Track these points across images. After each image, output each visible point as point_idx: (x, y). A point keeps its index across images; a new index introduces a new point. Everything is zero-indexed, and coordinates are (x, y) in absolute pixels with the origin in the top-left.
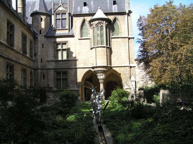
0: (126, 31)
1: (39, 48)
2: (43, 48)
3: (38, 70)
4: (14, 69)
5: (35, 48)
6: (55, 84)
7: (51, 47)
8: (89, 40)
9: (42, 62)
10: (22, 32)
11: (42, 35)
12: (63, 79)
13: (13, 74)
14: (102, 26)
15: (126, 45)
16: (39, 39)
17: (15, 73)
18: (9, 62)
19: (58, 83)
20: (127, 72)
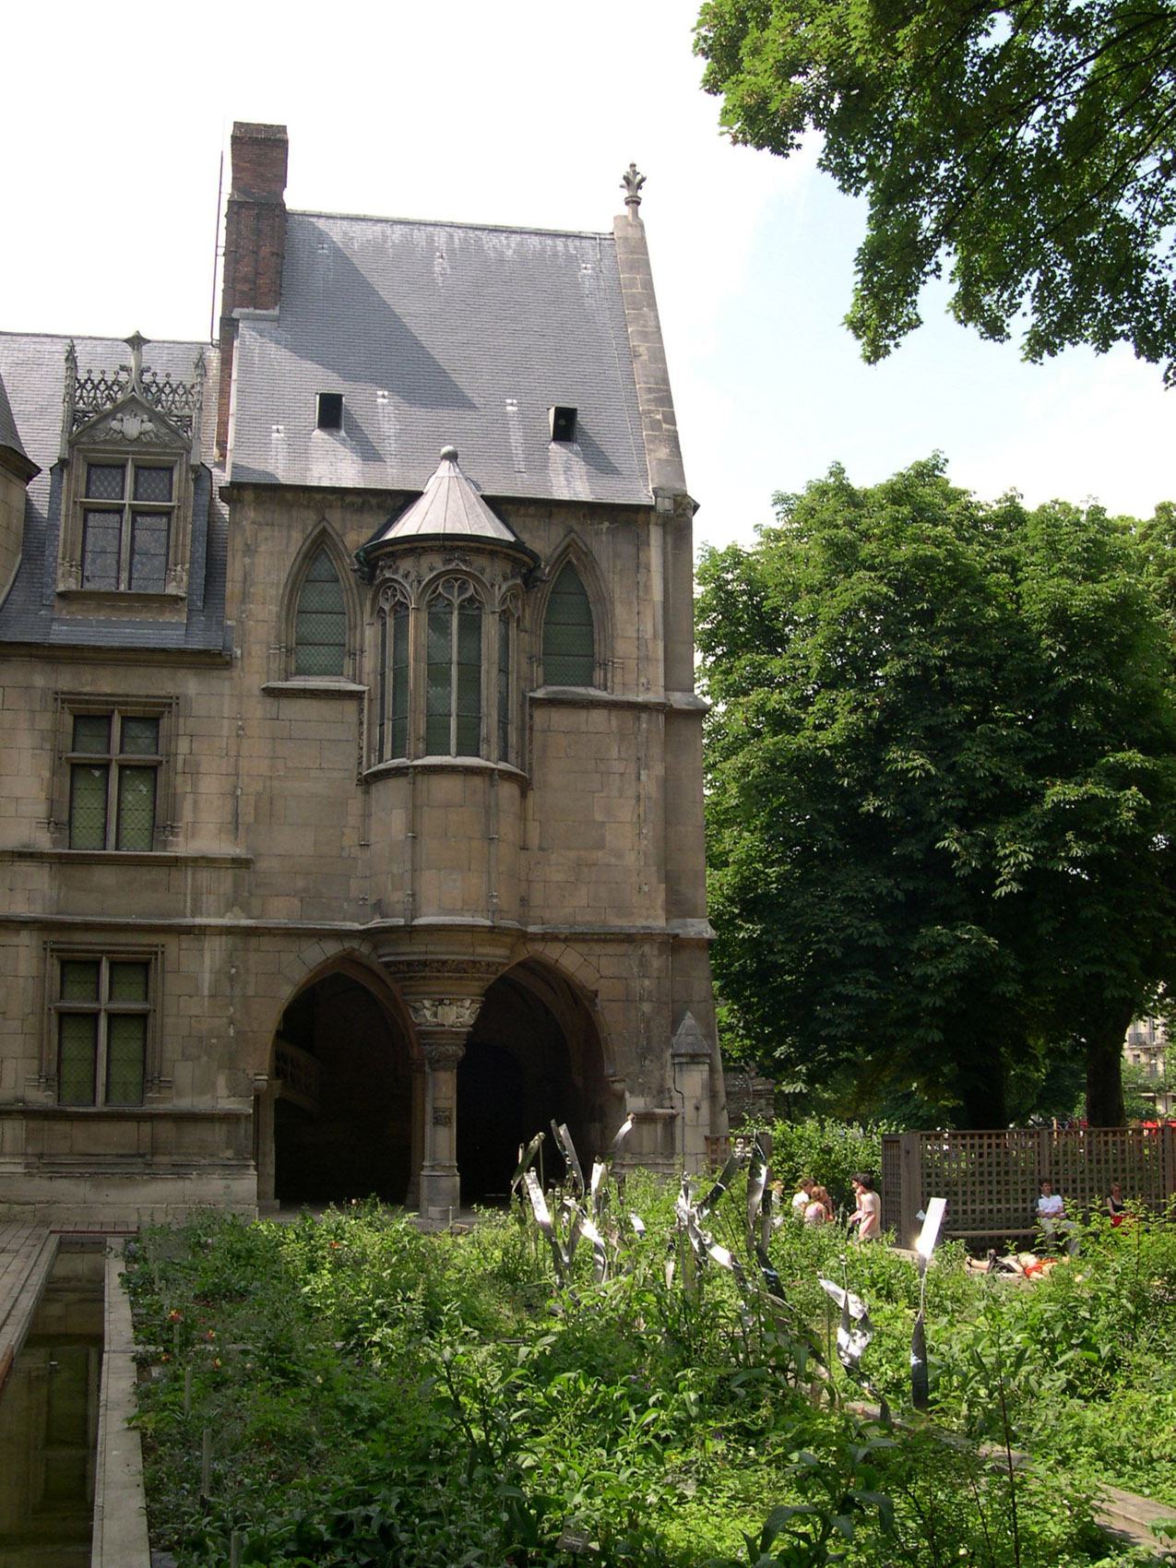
0: (647, 658)
6: (41, 1059)
7: (25, 740)
8: (350, 707)
12: (112, 1017)
14: (471, 600)
15: (647, 767)
19: (71, 1049)
20: (647, 982)
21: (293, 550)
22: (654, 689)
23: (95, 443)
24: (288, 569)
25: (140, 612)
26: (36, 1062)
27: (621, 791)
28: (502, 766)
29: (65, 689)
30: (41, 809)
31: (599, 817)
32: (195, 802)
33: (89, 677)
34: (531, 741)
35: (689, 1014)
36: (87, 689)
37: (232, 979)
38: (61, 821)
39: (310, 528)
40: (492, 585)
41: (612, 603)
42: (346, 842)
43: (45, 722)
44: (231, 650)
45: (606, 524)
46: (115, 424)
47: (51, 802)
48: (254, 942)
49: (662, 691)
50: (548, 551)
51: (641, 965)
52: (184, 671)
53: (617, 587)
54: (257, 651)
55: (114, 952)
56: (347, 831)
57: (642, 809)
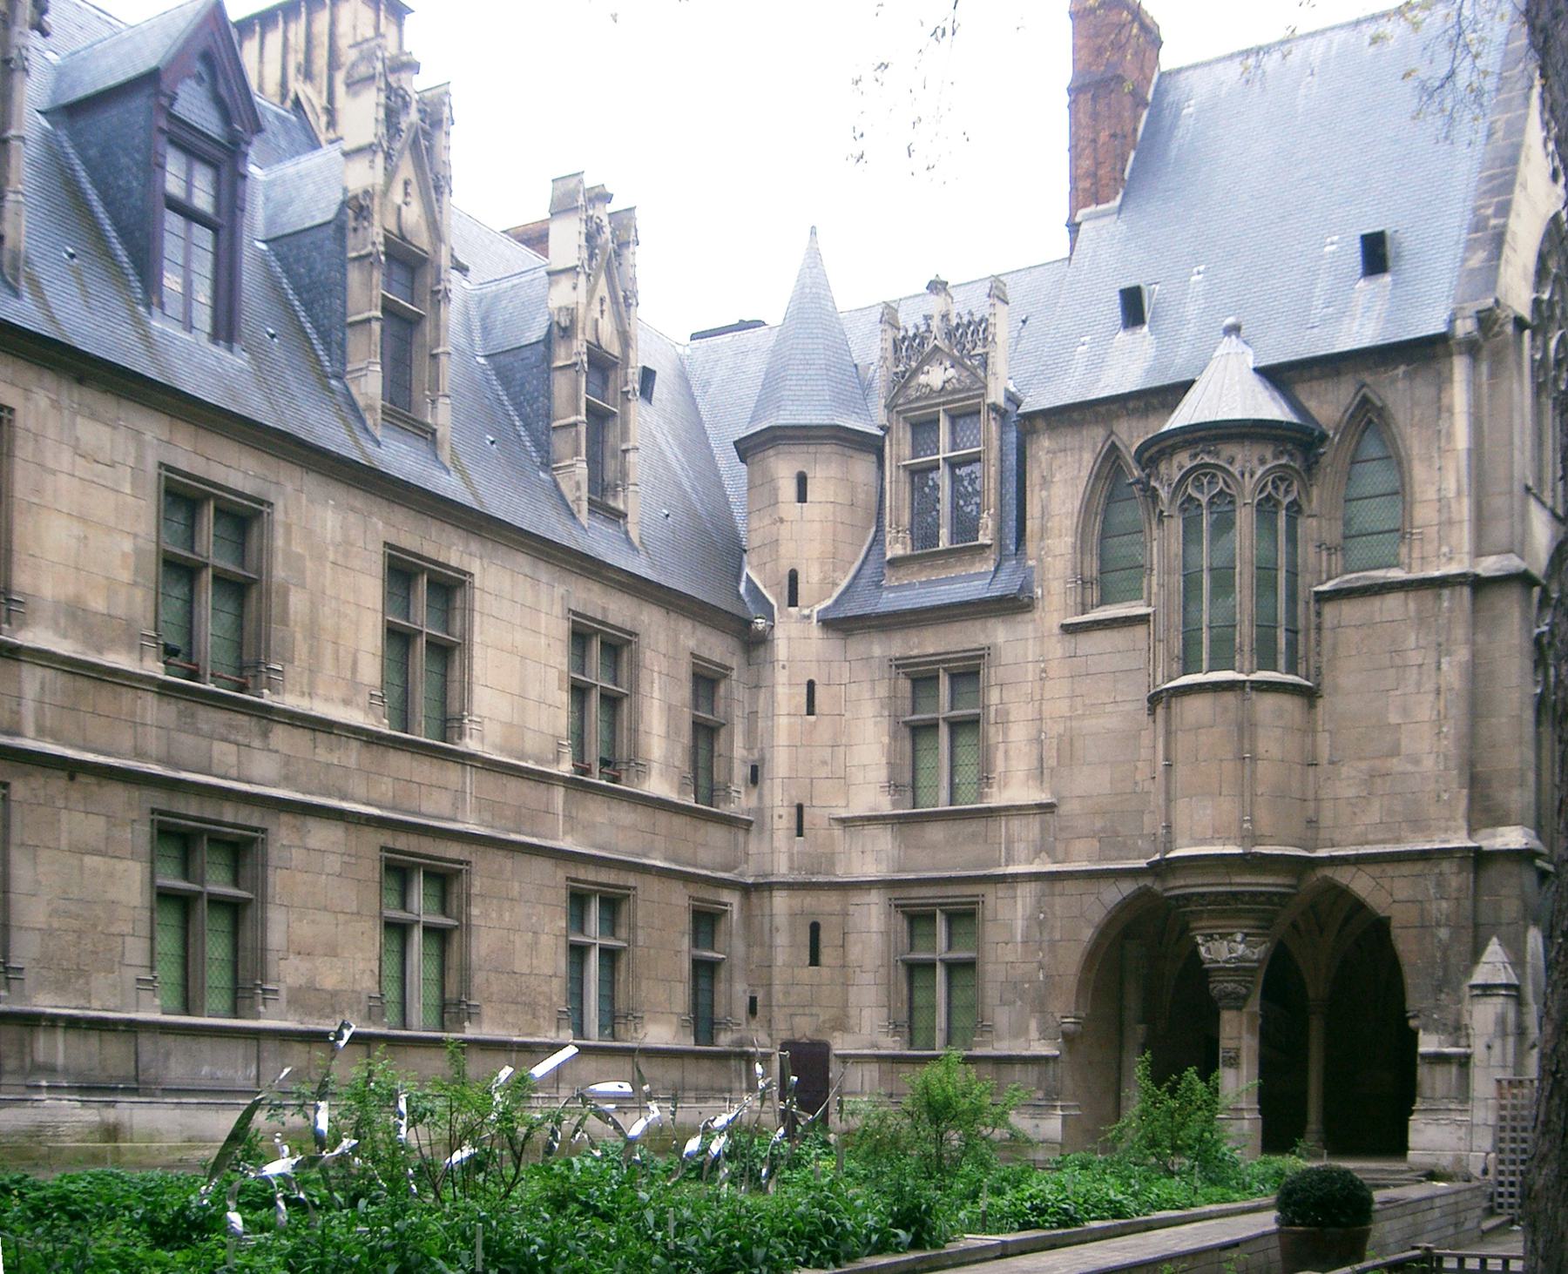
0: (1450, 522)
1: (783, 722)
2: (812, 718)
3: (771, 897)
4: (475, 891)
5: (753, 715)
8: (1140, 631)
9: (800, 833)
10: (575, 613)
11: (806, 612)
13: (466, 928)
15: (1449, 653)
16: (781, 649)
17: (474, 922)
18: (403, 842)
19: (920, 998)
20: (1444, 904)
21: (1085, 473)
22: (1457, 557)
23: (911, 402)
24: (1080, 496)
25: (954, 566)
26: (886, 1010)
27: (1419, 684)
28: (1290, 678)
29: (897, 655)
30: (882, 774)
31: (1394, 718)
32: (1006, 752)
33: (916, 640)
34: (1318, 643)
35: (1495, 940)
36: (915, 652)
37: (1041, 924)
38: (905, 782)
39: (1100, 445)
40: (1243, 475)
41: (1410, 462)
42: (1138, 778)
43: (882, 690)
44: (1032, 592)
45: (1402, 369)
46: (922, 379)
47: (891, 765)
48: (1058, 886)
49: (1466, 559)
50: (1338, 416)
51: (1439, 885)
52: (993, 620)
53: (1414, 443)
54: (1056, 586)
55: (946, 904)
56: (1140, 764)
57: (1442, 703)
